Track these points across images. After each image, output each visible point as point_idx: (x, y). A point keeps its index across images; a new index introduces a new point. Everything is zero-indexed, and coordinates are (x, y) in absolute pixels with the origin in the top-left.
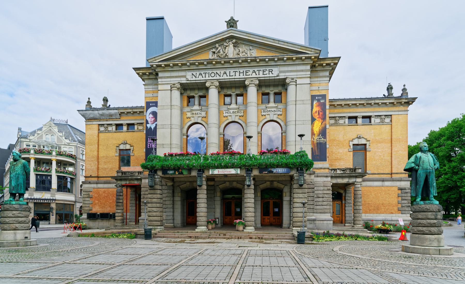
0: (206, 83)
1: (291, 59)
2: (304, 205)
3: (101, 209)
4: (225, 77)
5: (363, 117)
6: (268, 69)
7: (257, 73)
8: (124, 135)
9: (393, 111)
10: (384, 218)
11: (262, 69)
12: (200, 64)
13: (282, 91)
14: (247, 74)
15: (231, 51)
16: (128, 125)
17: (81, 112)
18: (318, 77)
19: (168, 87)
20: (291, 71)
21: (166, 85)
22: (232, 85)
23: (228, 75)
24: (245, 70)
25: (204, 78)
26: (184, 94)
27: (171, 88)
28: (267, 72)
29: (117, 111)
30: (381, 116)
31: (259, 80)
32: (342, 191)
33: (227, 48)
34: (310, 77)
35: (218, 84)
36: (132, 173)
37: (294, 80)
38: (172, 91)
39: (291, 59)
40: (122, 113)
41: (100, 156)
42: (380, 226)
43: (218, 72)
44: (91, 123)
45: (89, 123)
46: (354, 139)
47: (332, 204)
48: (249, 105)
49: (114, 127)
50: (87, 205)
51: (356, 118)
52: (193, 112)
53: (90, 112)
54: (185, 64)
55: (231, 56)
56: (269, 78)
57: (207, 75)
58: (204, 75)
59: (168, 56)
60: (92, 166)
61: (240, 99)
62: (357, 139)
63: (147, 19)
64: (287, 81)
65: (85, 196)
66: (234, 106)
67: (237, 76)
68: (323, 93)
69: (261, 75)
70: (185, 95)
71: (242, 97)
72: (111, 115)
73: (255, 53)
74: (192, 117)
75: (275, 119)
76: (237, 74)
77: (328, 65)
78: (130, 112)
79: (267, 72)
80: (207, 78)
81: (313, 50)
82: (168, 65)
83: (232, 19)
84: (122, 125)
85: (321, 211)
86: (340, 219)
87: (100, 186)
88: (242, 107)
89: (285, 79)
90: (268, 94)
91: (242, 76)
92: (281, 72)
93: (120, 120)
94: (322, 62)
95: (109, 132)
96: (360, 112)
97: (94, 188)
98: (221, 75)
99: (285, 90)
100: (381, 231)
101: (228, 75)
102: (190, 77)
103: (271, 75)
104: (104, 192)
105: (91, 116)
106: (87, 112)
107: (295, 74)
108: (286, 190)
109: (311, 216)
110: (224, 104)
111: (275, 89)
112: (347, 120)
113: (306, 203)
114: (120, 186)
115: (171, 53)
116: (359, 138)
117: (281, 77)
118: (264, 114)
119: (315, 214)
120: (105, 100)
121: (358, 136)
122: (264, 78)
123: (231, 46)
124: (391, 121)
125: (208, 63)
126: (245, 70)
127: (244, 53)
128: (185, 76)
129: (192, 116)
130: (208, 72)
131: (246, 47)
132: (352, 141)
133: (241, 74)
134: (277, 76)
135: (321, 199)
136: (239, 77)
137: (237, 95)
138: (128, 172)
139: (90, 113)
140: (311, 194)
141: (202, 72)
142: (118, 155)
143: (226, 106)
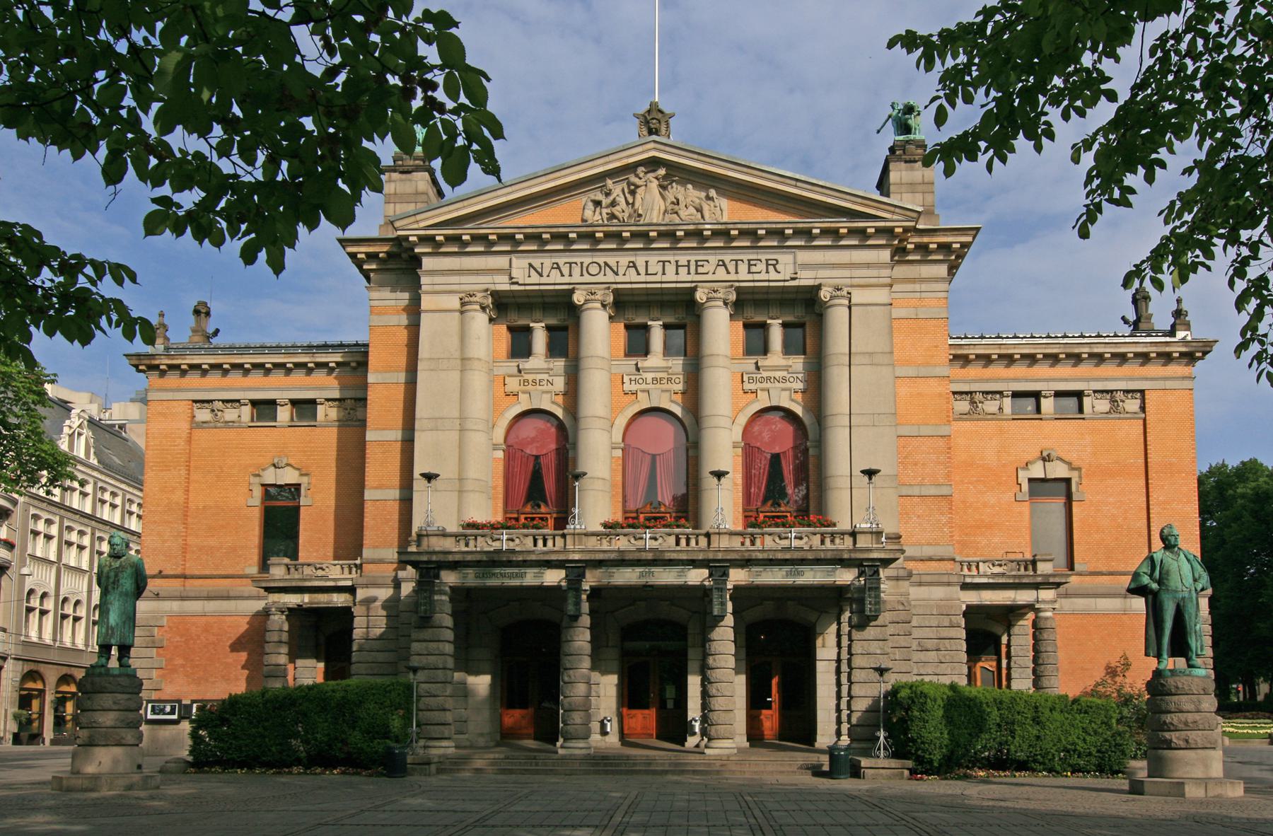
4: (632, 276)
5: (1059, 394)
6: (763, 257)
7: (731, 268)
9: (1147, 379)
11: (745, 257)
15: (652, 203)
19: (454, 302)
20: (834, 266)
21: (445, 297)
22: (652, 298)
23: (642, 271)
24: (693, 259)
25: (567, 279)
27: (463, 304)
28: (761, 267)
30: (1112, 391)
31: (738, 290)
37: (844, 293)
43: (612, 261)
49: (246, 411)
51: (1036, 395)
52: (526, 377)
56: (766, 284)
57: (576, 270)
58: (565, 270)
59: (457, 210)
64: (825, 294)
67: (670, 275)
69: (743, 274)
71: (682, 331)
73: (725, 211)
74: (524, 392)
75: (786, 403)
76: (670, 269)
80: (576, 278)
81: (897, 210)
83: (654, 109)
91: (683, 275)
94: (925, 240)
98: (621, 272)
101: (642, 271)
102: (525, 272)
103: (773, 275)
107: (846, 273)
112: (1007, 402)
115: (465, 203)
116: (1046, 459)
118: (753, 387)
121: (1045, 454)
122: (751, 284)
124: (1143, 409)
126: (693, 259)
129: (522, 387)
130: (578, 260)
133: (683, 271)
134: (793, 279)
135: (932, 656)
136: (674, 278)
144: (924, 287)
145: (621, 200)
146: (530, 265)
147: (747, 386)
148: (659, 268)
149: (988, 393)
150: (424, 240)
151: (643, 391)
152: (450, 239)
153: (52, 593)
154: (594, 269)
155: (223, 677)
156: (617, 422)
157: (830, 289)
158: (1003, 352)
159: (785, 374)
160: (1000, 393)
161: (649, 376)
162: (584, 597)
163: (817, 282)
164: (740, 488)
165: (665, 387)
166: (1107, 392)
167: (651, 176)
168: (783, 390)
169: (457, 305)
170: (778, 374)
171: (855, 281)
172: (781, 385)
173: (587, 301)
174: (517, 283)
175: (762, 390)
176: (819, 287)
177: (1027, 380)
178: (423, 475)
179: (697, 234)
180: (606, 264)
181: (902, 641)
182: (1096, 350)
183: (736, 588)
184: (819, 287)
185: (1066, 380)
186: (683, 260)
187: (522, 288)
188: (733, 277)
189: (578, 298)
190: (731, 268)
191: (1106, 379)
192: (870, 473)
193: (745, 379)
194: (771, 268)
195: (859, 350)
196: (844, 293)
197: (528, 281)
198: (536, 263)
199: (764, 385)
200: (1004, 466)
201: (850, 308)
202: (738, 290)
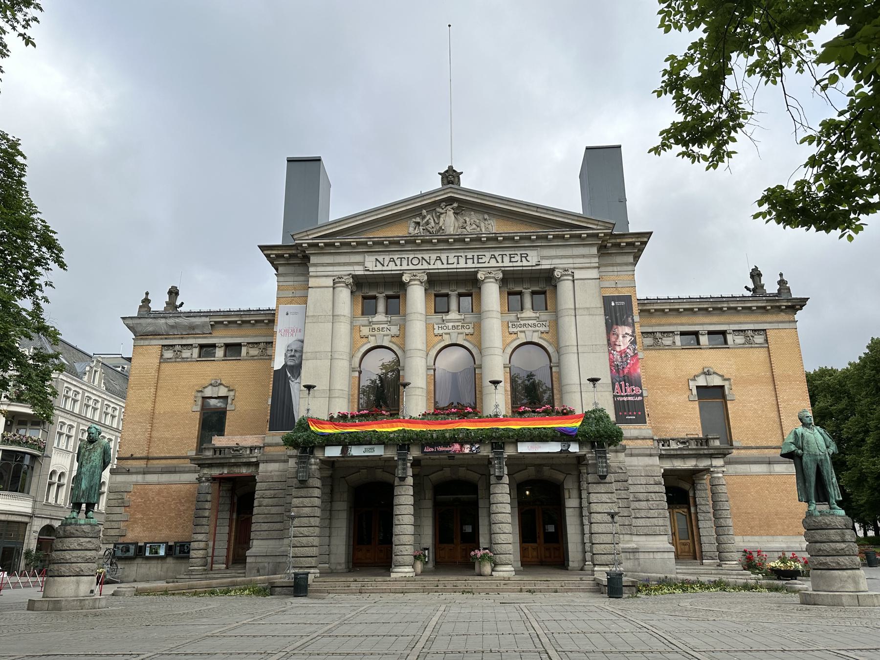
0: (402, 275)
1: (562, 237)
2: (613, 517)
3: (147, 533)
4: (439, 265)
5: (710, 333)
6: (519, 253)
7: (499, 259)
8: (219, 368)
10: (784, 545)
11: (508, 253)
12: (392, 243)
13: (547, 288)
14: (480, 261)
16: (227, 346)
17: (129, 322)
18: (612, 265)
19: (329, 282)
23: (445, 262)
25: (399, 268)
27: (334, 284)
28: (518, 258)
29: (207, 319)
31: (503, 272)
32: (686, 486)
33: (442, 216)
34: (598, 268)
35: (426, 278)
36: (237, 449)
38: (337, 290)
39: (562, 237)
40: (216, 322)
41: (157, 412)
42: (776, 564)
43: (426, 257)
44: (147, 342)
45: (142, 342)
46: (697, 376)
47: (668, 514)
48: (484, 315)
50: (115, 525)
51: (696, 334)
53: (150, 320)
54: (365, 244)
55: (451, 230)
57: (405, 262)
60: (136, 435)
61: (466, 301)
62: (703, 376)
63: (290, 161)
64: (557, 273)
65: (113, 502)
66: (453, 315)
67: (462, 264)
68: (625, 292)
69: (507, 263)
72: (192, 327)
77: (631, 245)
78: (235, 322)
80: (405, 267)
82: (332, 245)
84: (214, 346)
85: (646, 530)
86: (689, 548)
87: (152, 478)
88: (470, 317)
90: (520, 293)
91: (470, 264)
92: (543, 258)
93: (211, 337)
95: (184, 360)
96: (704, 324)
97: (136, 484)
98: (432, 263)
99: (551, 288)
100: (779, 574)
101: (445, 262)
102: (372, 264)
103: (525, 263)
104: (159, 493)
105: (150, 329)
106: (142, 321)
107: (571, 261)
108: (570, 485)
109: (628, 542)
110: (435, 312)
112: (678, 339)
113: (617, 513)
114: (207, 480)
117: (543, 267)
119: (635, 538)
120: (173, 293)
123: (451, 213)
124: (766, 341)
125: (407, 242)
126: (475, 254)
127: (474, 226)
130: (406, 256)
131: (477, 215)
132: (694, 380)
136: (465, 266)
137: (460, 295)
138: (229, 448)
139: (149, 324)
140: (623, 494)
141: (395, 257)
142: (198, 408)
143: (439, 316)
144: (619, 268)
147: (511, 330)
148: (455, 260)
149: (664, 332)
150: (310, 245)
151: (446, 334)
152: (326, 245)
153: (67, 474)
154: (415, 261)
155: (167, 526)
156: (430, 353)
159: (535, 322)
160: (673, 332)
161: (450, 325)
162: (409, 465)
163: (552, 267)
164: (509, 393)
165: (460, 331)
166: (742, 331)
169: (332, 284)
170: (530, 322)
171: (576, 266)
173: (411, 280)
175: (521, 332)
176: (553, 270)
177: (689, 325)
178: (305, 386)
179: (478, 239)
181: (623, 494)
183: (509, 457)
184: (553, 270)
185: (714, 324)
186: (470, 255)
188: (500, 264)
189: (406, 278)
190: (499, 259)
191: (741, 323)
192: (594, 381)
193: (510, 325)
194: (524, 259)
195: (581, 306)
198: (380, 258)
200: (679, 378)
201: (573, 281)
202: (503, 272)
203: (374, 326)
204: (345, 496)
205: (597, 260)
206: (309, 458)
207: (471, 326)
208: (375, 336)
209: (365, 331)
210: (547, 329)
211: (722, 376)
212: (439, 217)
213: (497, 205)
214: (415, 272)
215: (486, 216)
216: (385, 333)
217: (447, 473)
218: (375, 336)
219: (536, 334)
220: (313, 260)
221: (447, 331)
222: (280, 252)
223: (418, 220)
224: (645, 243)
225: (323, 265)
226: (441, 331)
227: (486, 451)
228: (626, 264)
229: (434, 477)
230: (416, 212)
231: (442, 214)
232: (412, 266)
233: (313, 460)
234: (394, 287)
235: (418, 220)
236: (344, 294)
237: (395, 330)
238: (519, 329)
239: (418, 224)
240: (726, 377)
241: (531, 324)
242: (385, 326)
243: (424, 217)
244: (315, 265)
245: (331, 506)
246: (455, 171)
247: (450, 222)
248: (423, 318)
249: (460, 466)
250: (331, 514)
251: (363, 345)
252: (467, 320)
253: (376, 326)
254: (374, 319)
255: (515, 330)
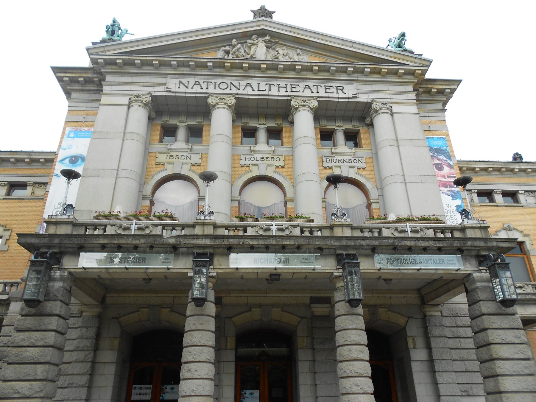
4: (249, 91)
6: (334, 85)
7: (314, 89)
11: (323, 85)
14: (294, 90)
19: (125, 100)
25: (204, 91)
26: (156, 121)
27: (130, 103)
28: (333, 90)
38: (133, 109)
43: (236, 83)
57: (211, 87)
67: (274, 91)
69: (322, 93)
70: (159, 123)
79: (333, 90)
80: (211, 90)
89: (368, 105)
91: (283, 92)
98: (242, 88)
101: (256, 88)
102: (175, 86)
103: (341, 95)
107: (388, 96)
111: (346, 123)
117: (360, 100)
128: (163, 85)
134: (354, 97)
136: (277, 93)
145: (242, 50)
146: (180, 82)
147: (325, 164)
152: (126, 63)
157: (380, 104)
158: (469, 166)
159: (350, 158)
161: (259, 156)
163: (369, 100)
167: (260, 39)
168: (350, 167)
169: (127, 103)
170: (345, 158)
172: (349, 164)
174: (170, 91)
175: (336, 167)
177: (485, 184)
180: (231, 83)
182: (523, 167)
185: (508, 184)
186: (282, 84)
187: (174, 94)
188: (315, 94)
189: (211, 101)
191: (530, 185)
193: (324, 159)
194: (339, 91)
196: (388, 106)
197: (178, 90)
198: (185, 81)
199: (337, 164)
201: (392, 115)
203: (172, 154)
204: (116, 342)
205: (414, 97)
206: (49, 268)
207: (282, 158)
208: (172, 163)
209: (162, 158)
210: (363, 165)
211: (521, 232)
212: (250, 48)
213: (311, 39)
214: (222, 96)
215: (299, 51)
216: (185, 161)
217: (256, 313)
218: (172, 163)
219: (351, 169)
220: (109, 78)
221: (255, 162)
222: (74, 75)
223: (227, 48)
224: (453, 91)
225: (119, 84)
226: (248, 162)
227: (325, 265)
228: (437, 110)
229: (239, 320)
230: (226, 40)
231: (253, 44)
232: (222, 91)
233: (58, 274)
234: (199, 110)
235: (227, 48)
236: (139, 116)
237: (196, 159)
238: (333, 164)
239: (227, 52)
240: (526, 232)
241: (345, 159)
242: (185, 154)
243: (234, 47)
244: (111, 83)
245: (95, 356)
246: (266, 10)
247: (260, 51)
248: (229, 141)
249: (272, 306)
250: (93, 368)
251: (159, 172)
252: (277, 153)
253: (174, 154)
254: (173, 146)
255: (329, 164)
